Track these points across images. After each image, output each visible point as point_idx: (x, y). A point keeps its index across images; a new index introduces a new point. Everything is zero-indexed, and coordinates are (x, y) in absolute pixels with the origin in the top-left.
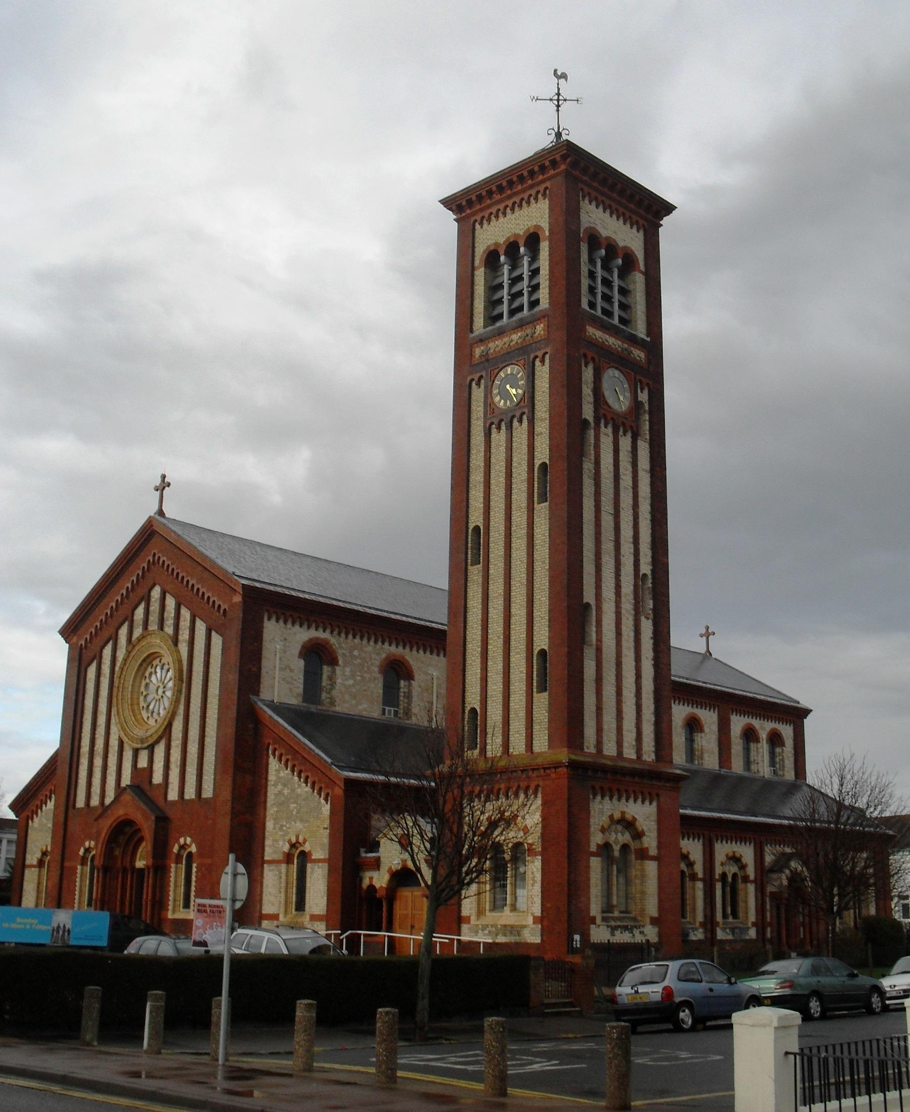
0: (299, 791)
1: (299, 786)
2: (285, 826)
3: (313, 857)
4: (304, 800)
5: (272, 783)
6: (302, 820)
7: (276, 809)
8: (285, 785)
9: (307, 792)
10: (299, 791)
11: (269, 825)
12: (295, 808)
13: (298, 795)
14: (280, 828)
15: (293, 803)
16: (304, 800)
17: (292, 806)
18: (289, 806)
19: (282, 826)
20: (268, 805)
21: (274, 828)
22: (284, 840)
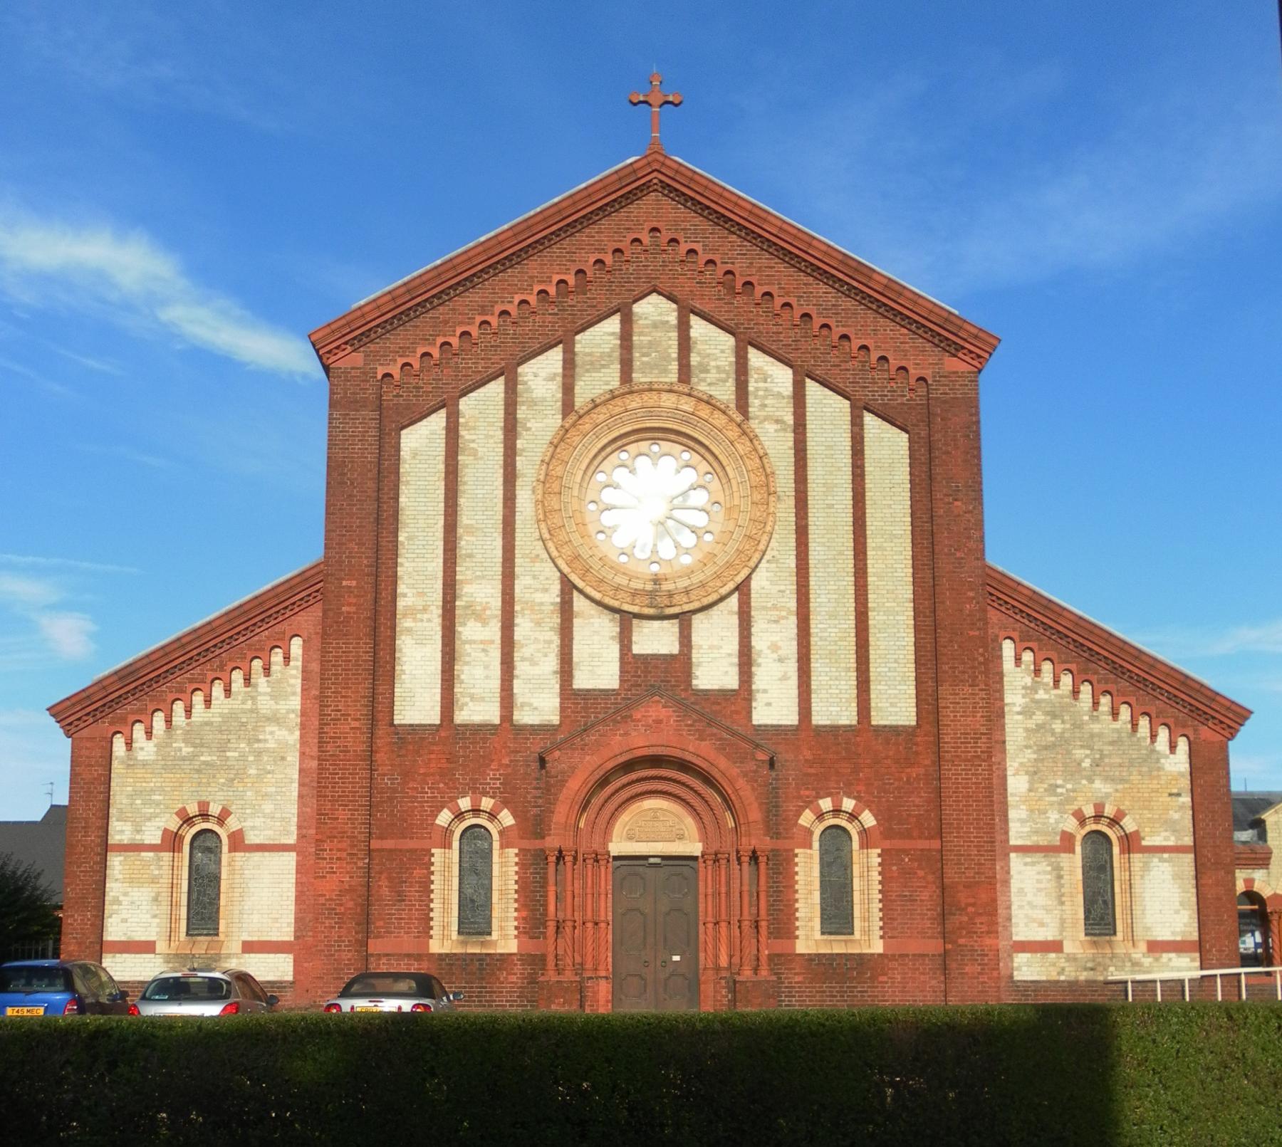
0: (1096, 727)
1: (1094, 719)
2: (1057, 786)
3: (1144, 843)
4: (1112, 743)
5: (1018, 709)
6: (1108, 779)
7: (1035, 756)
8: (1054, 715)
9: (1118, 731)
10: (1096, 727)
11: (1017, 784)
12: (1087, 756)
13: (1092, 736)
14: (1046, 790)
15: (1082, 747)
16: (1112, 743)
17: (1079, 753)
18: (1069, 752)
19: (1057, 786)
20: (1010, 747)
21: (1030, 790)
22: (1061, 812)
